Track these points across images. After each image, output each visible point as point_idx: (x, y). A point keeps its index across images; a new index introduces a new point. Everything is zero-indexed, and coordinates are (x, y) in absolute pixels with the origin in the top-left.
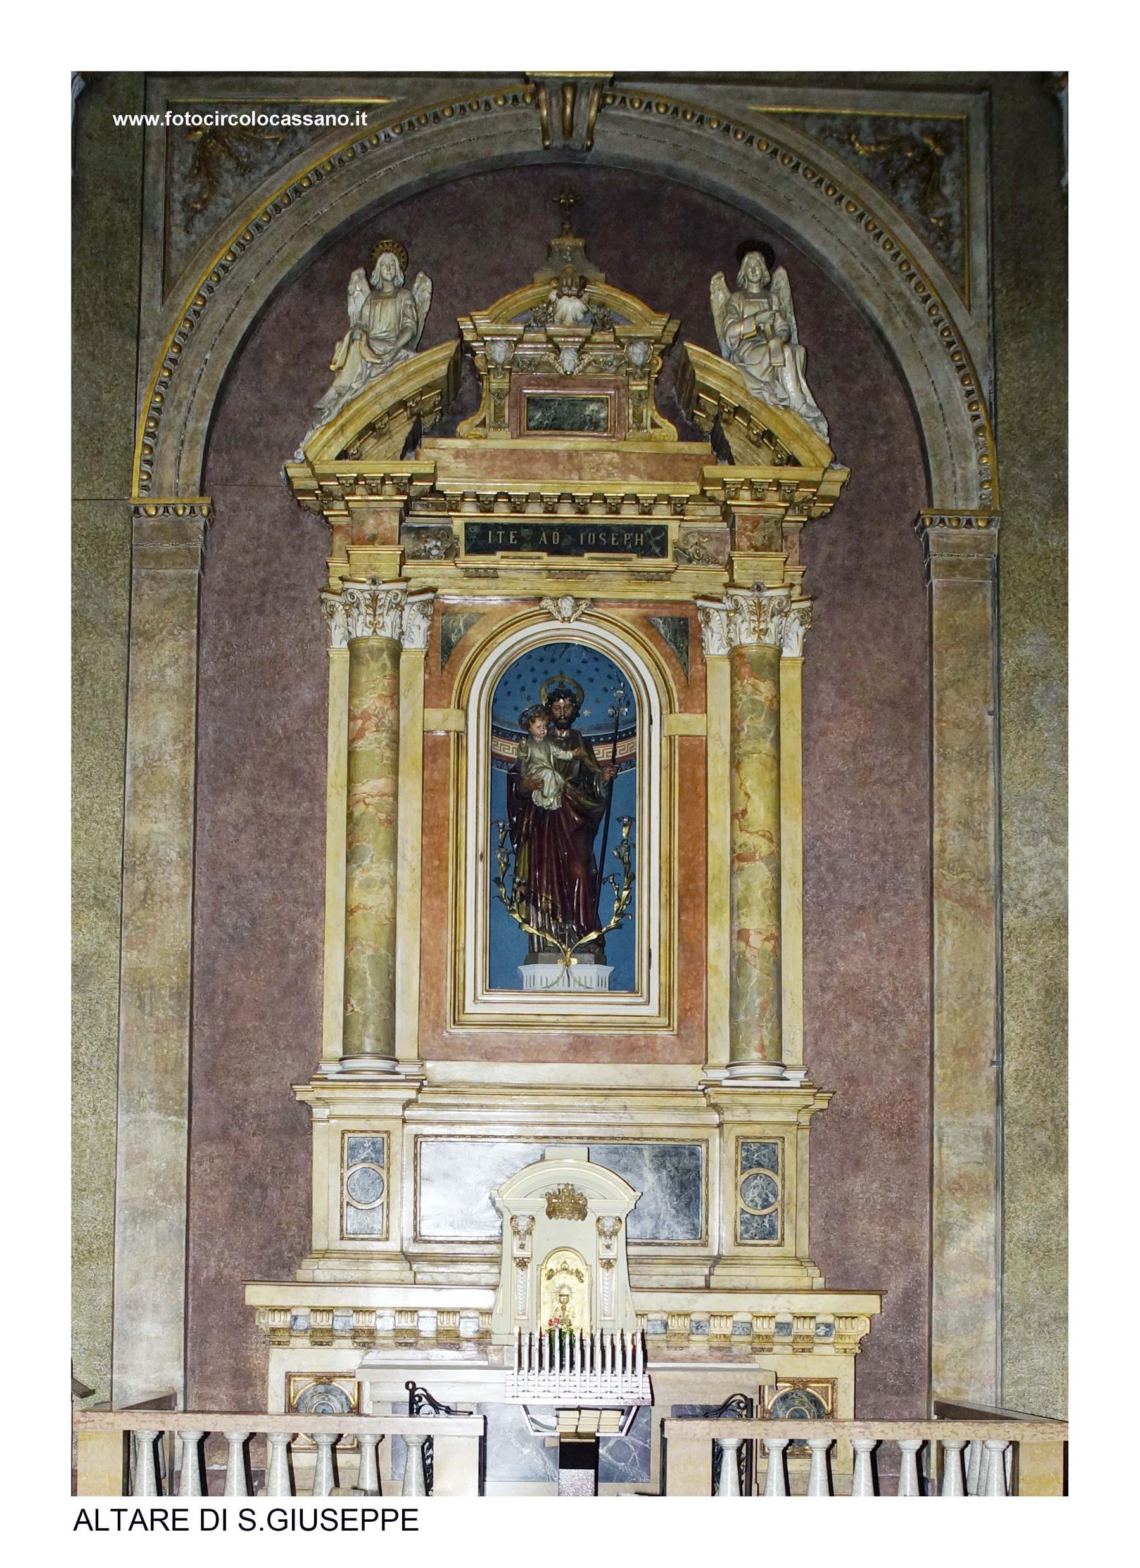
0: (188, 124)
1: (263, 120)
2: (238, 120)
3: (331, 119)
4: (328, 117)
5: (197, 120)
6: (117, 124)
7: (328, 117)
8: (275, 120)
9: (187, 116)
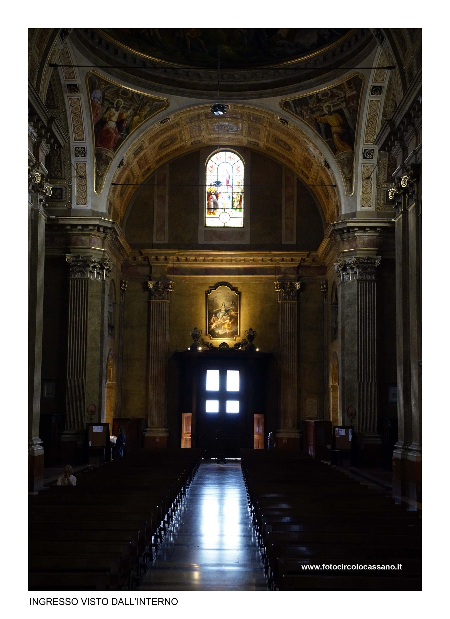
0: (331, 569)
1: (361, 567)
2: (351, 567)
3: (388, 567)
4: (386, 566)
5: (335, 567)
6: (303, 569)
7: (386, 566)
8: (365, 567)
9: (331, 565)
